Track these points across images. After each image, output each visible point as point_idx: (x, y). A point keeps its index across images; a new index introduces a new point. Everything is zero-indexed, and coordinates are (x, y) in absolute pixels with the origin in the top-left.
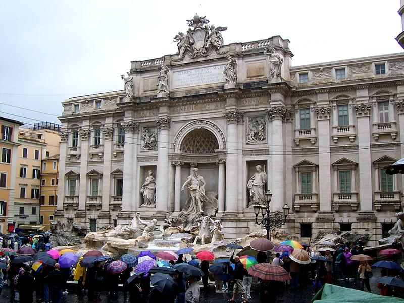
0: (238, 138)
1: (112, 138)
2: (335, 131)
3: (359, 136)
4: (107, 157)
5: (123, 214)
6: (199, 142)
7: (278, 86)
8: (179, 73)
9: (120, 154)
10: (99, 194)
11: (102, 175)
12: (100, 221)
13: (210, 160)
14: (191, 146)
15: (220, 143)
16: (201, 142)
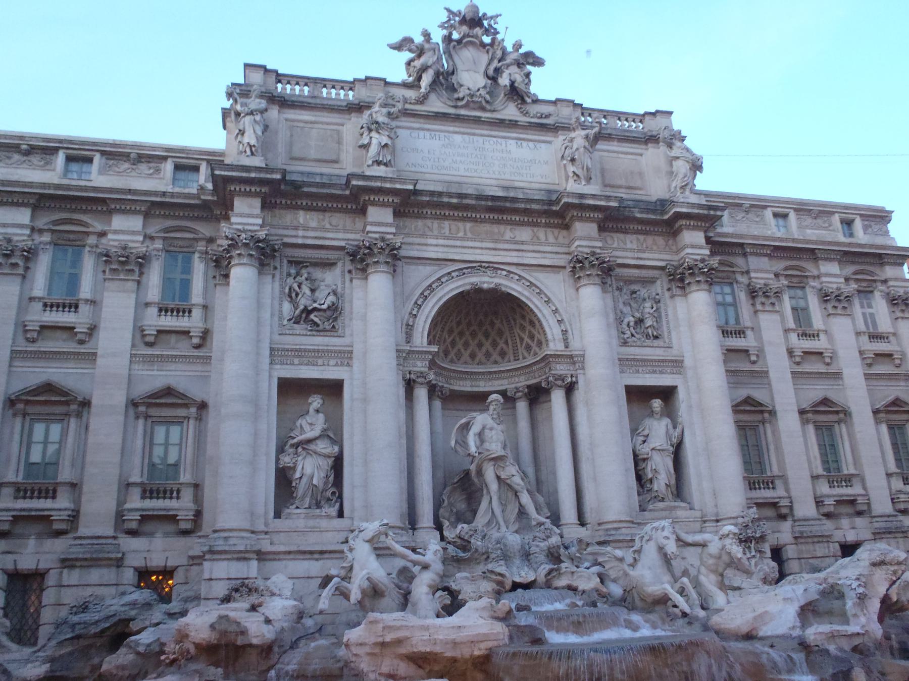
0: (608, 325)
1: (139, 282)
2: (793, 337)
3: (841, 353)
4: (115, 340)
5: (231, 542)
6: (451, 332)
7: (712, 212)
8: (415, 134)
9: (173, 338)
10: (65, 474)
11: (86, 404)
12: (72, 577)
13: (482, 383)
14: (434, 336)
15: (552, 330)
16: (455, 334)
